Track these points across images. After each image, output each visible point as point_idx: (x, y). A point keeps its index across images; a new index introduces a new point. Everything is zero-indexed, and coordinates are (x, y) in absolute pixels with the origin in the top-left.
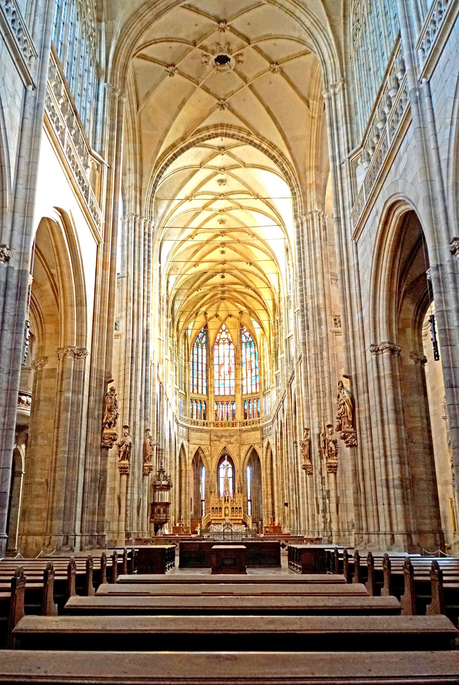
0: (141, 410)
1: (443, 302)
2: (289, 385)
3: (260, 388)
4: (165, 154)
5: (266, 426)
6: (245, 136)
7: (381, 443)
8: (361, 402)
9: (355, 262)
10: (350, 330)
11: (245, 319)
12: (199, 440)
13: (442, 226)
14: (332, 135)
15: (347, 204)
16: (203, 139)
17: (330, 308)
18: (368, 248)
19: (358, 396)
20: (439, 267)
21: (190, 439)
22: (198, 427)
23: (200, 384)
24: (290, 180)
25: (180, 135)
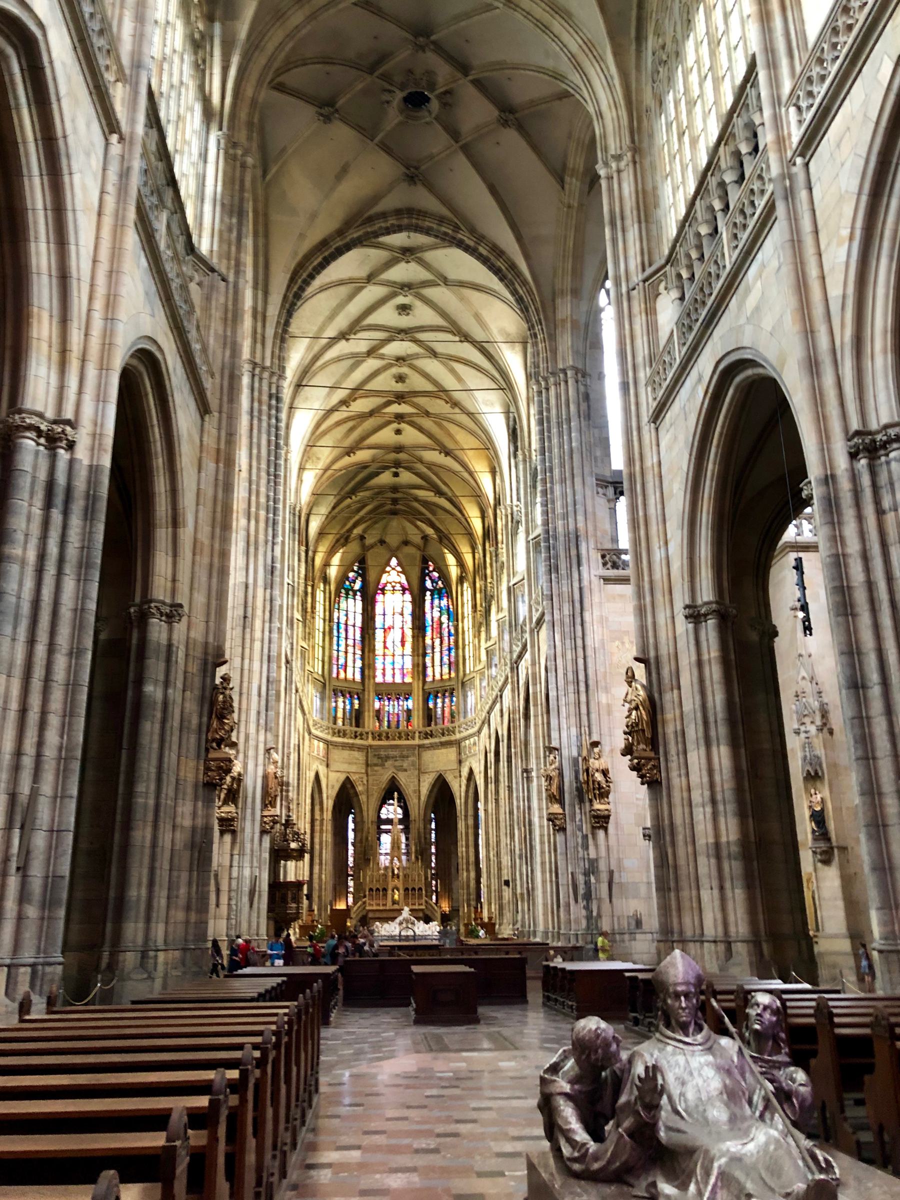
0: (259, 713)
2: (515, 666)
3: (457, 671)
4: (308, 257)
5: (465, 738)
6: (450, 232)
7: (705, 779)
8: (668, 706)
9: (655, 460)
10: (646, 578)
11: (431, 551)
12: (347, 765)
14: (614, 241)
15: (640, 359)
16: (376, 235)
17: (596, 536)
18: (681, 438)
19: (660, 694)
20: (829, 479)
21: (331, 762)
22: (345, 740)
23: (350, 663)
24: (527, 311)
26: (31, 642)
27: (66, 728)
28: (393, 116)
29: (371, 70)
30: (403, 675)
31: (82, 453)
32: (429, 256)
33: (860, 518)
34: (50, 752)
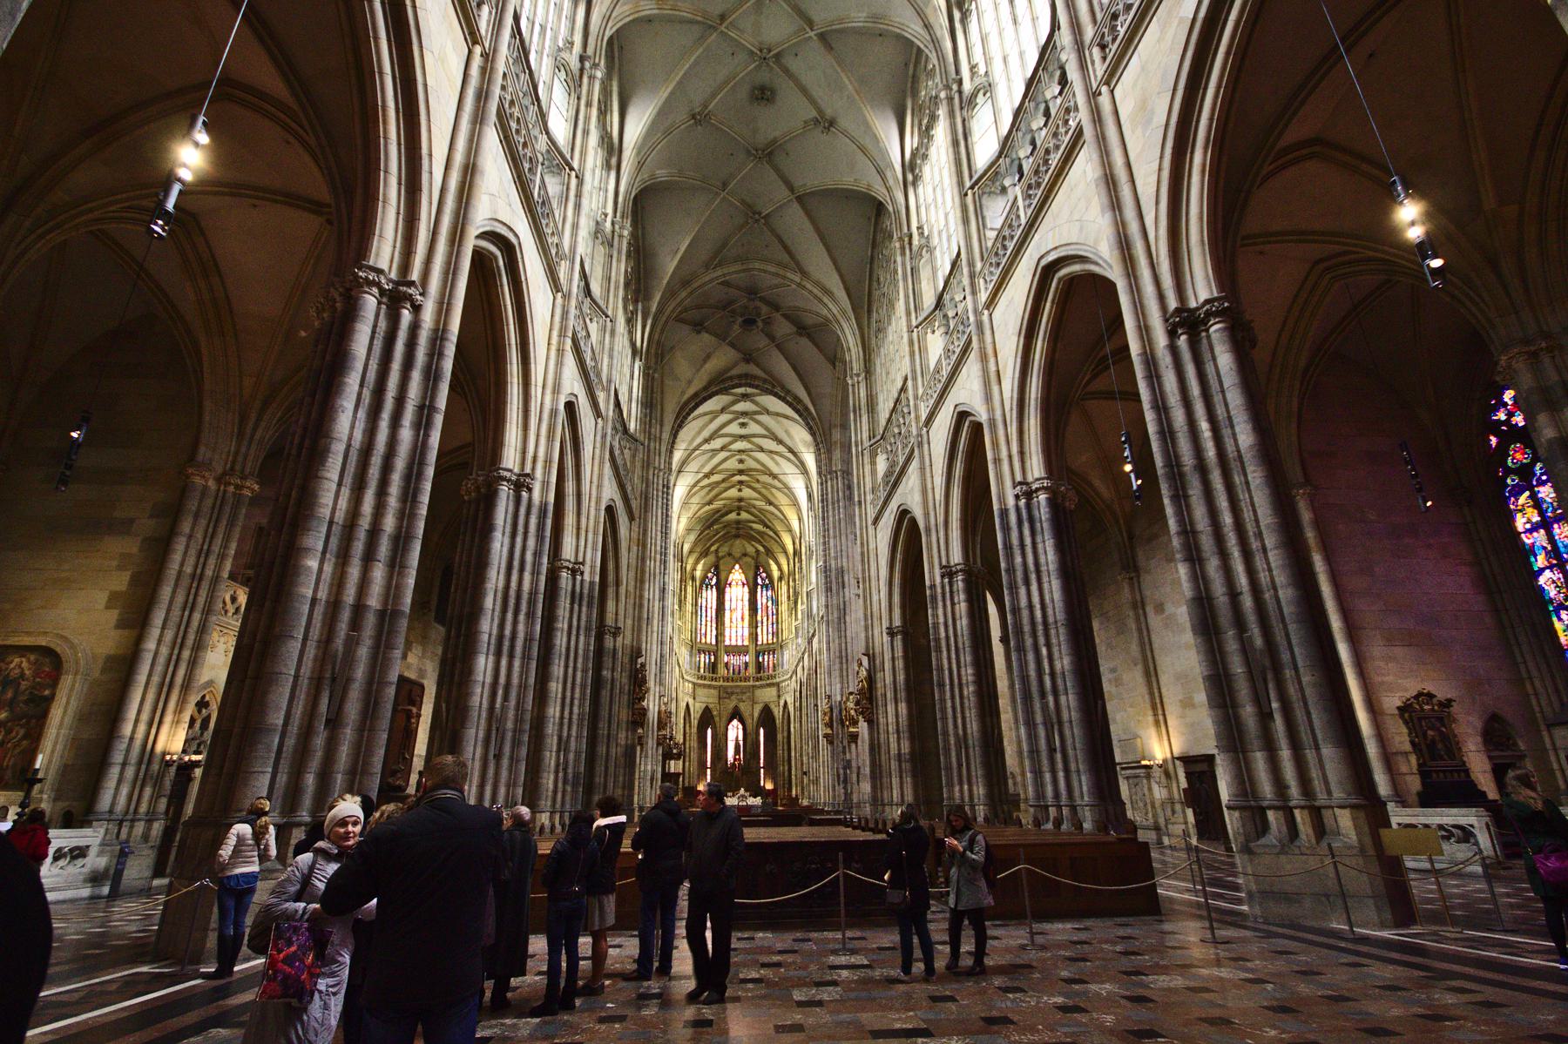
1: (935, 616)
2: (810, 642)
11: (762, 558)
12: (707, 697)
20: (933, 586)
27: (581, 705)
28: (737, 328)
29: (724, 308)
31: (587, 577)
34: (575, 717)
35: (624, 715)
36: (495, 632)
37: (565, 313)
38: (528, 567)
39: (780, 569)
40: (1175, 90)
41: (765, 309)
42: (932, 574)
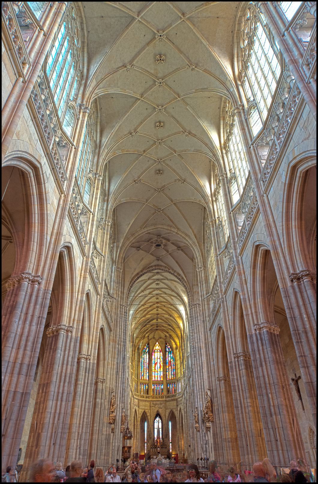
2: (189, 380)
4: (134, 277)
11: (168, 340)
12: (145, 406)
13: (231, 348)
20: (231, 362)
25: (140, 270)
26: (82, 401)
28: (153, 248)
30: (160, 378)
31: (92, 361)
32: (163, 274)
33: (236, 371)
34: (85, 423)
35: (106, 420)
36: (56, 391)
37: (87, 263)
38: (70, 363)
39: (176, 344)
40: (283, 202)
41: (164, 241)
42: (231, 358)
